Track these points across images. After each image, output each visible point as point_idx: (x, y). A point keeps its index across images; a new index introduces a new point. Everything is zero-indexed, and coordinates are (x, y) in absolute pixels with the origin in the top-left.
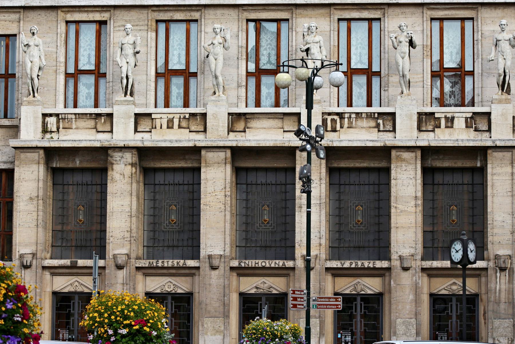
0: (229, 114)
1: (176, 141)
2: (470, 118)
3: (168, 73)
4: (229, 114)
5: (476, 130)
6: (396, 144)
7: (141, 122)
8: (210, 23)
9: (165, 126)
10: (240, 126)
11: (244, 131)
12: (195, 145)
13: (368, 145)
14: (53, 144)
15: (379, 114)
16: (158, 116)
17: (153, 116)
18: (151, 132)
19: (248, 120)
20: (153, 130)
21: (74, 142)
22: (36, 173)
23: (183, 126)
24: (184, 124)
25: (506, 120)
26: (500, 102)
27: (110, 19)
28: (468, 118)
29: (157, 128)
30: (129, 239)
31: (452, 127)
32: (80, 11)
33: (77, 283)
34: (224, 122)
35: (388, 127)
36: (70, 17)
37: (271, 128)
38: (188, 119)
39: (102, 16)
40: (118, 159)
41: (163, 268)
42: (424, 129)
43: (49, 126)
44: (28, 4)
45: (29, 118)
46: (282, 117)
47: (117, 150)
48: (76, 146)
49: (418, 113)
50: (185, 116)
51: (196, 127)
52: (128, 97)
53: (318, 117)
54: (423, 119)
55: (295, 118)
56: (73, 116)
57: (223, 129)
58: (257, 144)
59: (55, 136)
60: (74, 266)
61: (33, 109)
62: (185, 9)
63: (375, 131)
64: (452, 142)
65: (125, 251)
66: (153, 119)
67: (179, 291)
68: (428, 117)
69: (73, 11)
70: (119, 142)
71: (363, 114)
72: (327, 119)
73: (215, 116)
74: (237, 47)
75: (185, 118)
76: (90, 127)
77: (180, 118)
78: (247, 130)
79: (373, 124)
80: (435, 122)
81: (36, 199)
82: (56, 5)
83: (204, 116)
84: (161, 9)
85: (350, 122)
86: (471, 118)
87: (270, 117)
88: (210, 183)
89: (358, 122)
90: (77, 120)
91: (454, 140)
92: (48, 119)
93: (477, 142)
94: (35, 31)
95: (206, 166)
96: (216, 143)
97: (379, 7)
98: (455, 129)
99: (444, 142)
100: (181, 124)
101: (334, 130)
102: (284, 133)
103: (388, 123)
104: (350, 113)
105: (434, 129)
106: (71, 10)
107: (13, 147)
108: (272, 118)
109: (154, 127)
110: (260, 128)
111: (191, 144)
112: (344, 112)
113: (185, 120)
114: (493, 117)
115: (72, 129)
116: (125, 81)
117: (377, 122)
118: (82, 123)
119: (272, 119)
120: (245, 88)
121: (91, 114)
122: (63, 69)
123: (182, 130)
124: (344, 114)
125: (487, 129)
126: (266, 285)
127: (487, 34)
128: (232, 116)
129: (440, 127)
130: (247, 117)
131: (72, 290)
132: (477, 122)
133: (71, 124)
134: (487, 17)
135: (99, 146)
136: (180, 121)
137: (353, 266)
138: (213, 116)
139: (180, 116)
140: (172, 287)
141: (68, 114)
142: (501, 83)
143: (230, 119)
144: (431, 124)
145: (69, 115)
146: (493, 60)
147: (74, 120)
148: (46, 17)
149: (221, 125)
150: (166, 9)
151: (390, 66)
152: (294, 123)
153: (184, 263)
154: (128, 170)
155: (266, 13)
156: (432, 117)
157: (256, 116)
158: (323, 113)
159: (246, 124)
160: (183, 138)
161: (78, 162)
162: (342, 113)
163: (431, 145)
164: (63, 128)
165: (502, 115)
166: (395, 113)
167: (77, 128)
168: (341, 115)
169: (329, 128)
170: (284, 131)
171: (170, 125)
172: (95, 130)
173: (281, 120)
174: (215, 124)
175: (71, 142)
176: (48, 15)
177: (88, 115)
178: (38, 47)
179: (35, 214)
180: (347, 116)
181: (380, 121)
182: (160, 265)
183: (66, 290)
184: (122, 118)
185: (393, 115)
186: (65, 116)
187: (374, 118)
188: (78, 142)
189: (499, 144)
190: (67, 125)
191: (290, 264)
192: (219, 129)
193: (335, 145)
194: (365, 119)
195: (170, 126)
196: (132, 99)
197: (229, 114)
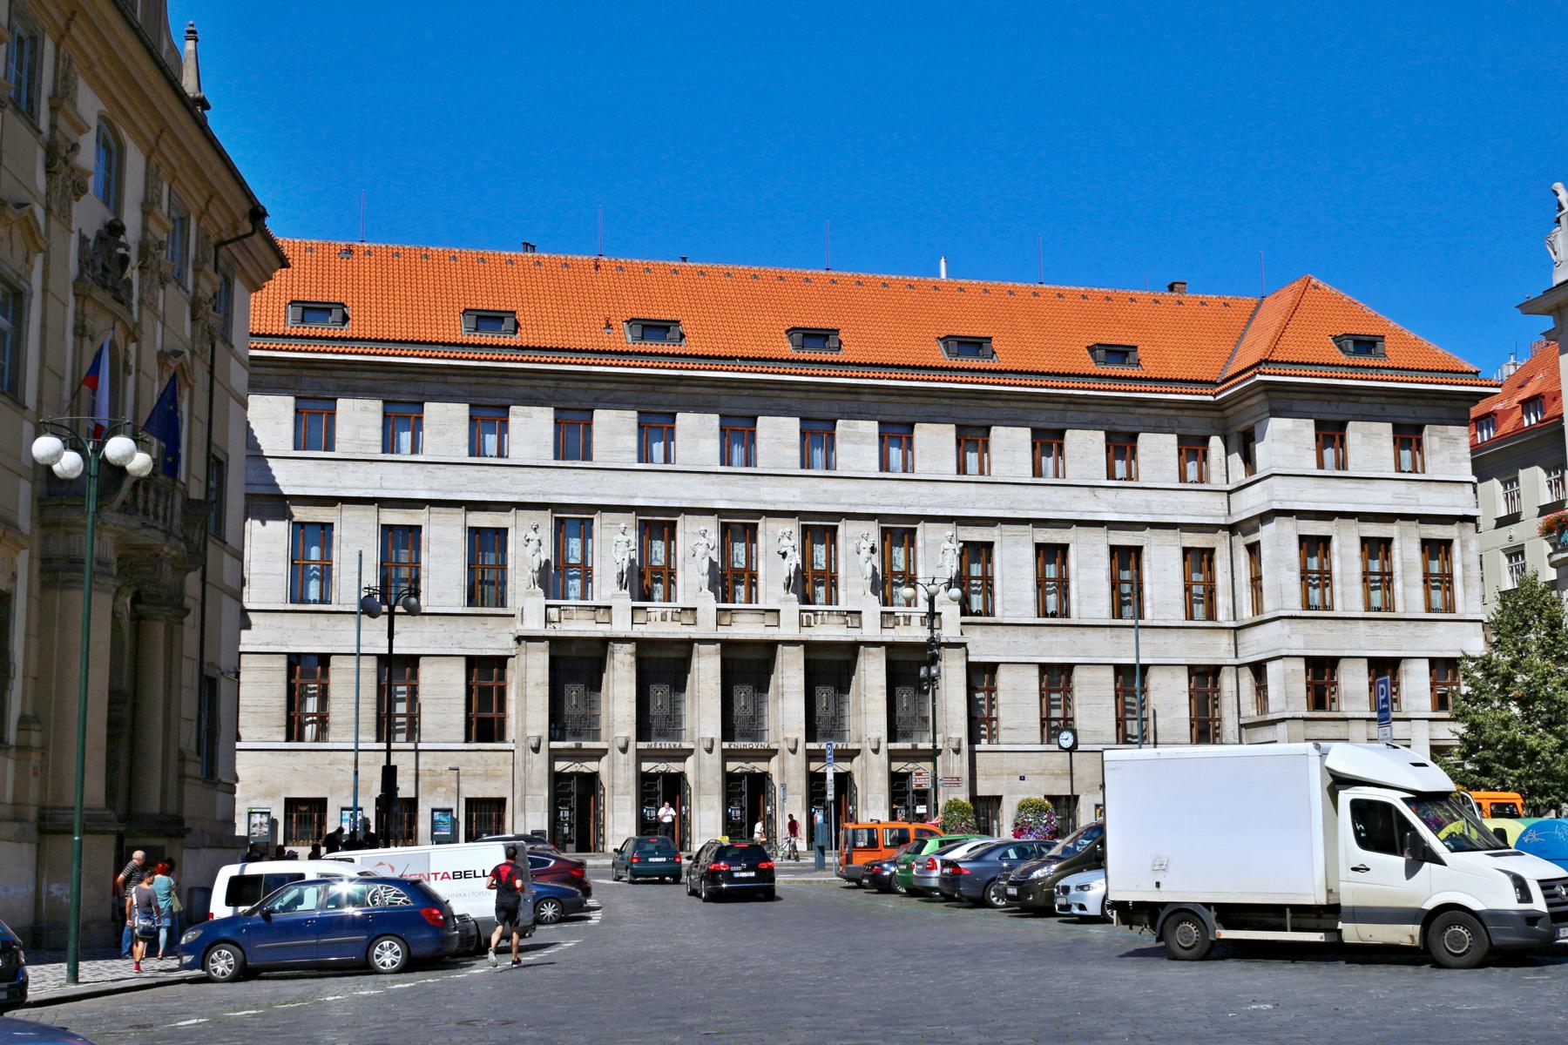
9: (659, 619)
10: (726, 620)
24: (676, 617)
55: (775, 614)
59: (557, 626)
65: (626, 735)
67: (673, 771)
85: (823, 619)
92: (549, 610)
101: (809, 626)
111: (686, 636)
129: (899, 624)
160: (675, 630)
161: (574, 650)
181: (848, 618)
182: (658, 747)
189: (952, 640)
190: (568, 616)
195: (664, 618)
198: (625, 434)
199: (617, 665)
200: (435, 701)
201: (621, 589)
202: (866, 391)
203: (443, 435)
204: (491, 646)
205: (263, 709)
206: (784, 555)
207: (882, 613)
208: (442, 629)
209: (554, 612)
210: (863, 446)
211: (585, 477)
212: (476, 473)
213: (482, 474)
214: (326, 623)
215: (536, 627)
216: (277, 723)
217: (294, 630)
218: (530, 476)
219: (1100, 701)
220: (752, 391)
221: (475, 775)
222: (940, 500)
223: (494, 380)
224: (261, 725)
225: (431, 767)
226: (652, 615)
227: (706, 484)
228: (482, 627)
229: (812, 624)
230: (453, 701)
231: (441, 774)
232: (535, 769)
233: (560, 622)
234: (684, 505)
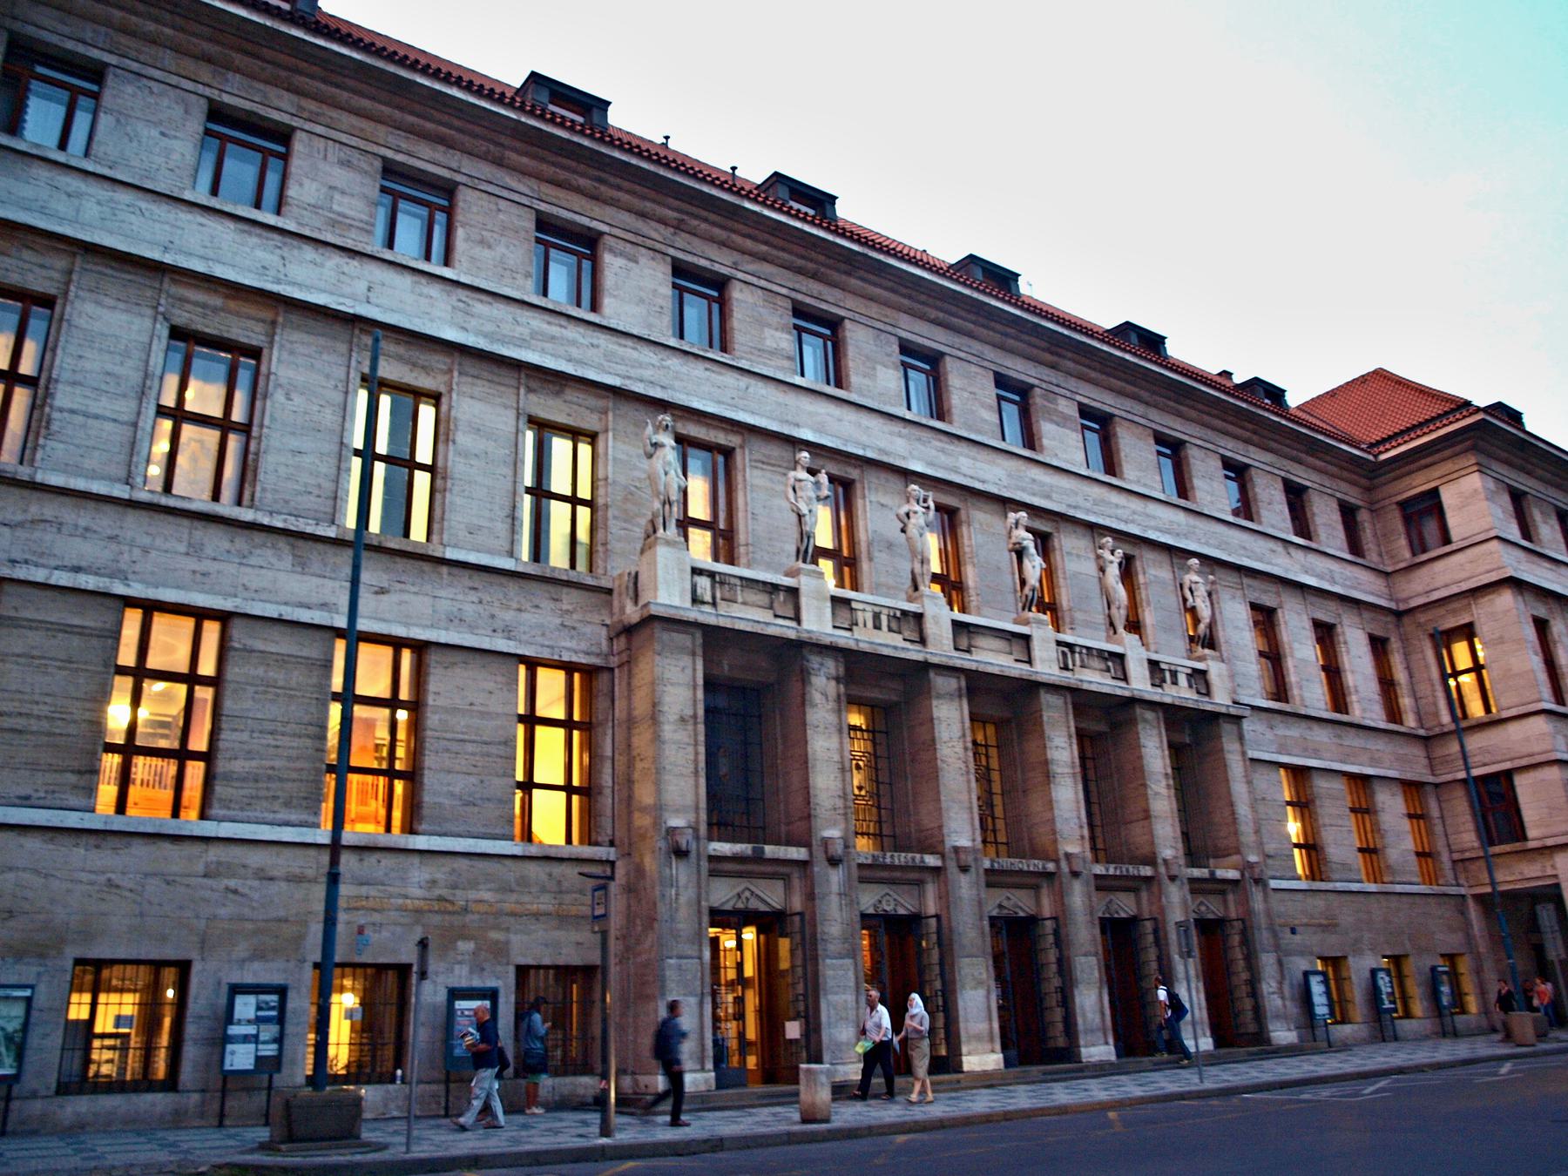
9: (870, 624)
11: (968, 651)
14: (723, 622)
17: (854, 605)
20: (855, 628)
22: (689, 671)
24: (894, 625)
30: (841, 811)
32: (699, 422)
33: (747, 894)
40: (816, 666)
41: (892, 867)
47: (815, 649)
55: (1022, 642)
56: (738, 582)
60: (758, 858)
66: (852, 609)
67: (901, 911)
75: (895, 616)
76: (760, 603)
79: (1103, 666)
81: (691, 721)
85: (1082, 661)
88: (944, 725)
95: (939, 697)
121: (764, 583)
126: (1012, 902)
131: (740, 905)
133: (735, 594)
137: (1118, 873)
140: (892, 903)
153: (922, 861)
154: (832, 688)
161: (726, 667)
164: (723, 599)
167: (744, 603)
175: (751, 624)
179: (691, 749)
180: (1077, 649)
182: (888, 860)
183: (728, 907)
190: (727, 595)
191: (1051, 867)
198: (777, 329)
199: (817, 697)
200: (455, 747)
202: (1070, 355)
203: (490, 247)
204: (568, 644)
205: (45, 725)
208: (473, 597)
209: (704, 583)
210: (1068, 432)
211: (721, 378)
212: (545, 326)
213: (554, 330)
214: (226, 545)
215: (676, 602)
216: (76, 764)
217: (145, 551)
218: (635, 354)
219: (1340, 822)
220: (941, 315)
221: (537, 916)
222: (1153, 523)
223: (583, 182)
224: (33, 766)
225: (444, 892)
226: (860, 615)
227: (891, 434)
228: (552, 605)
229: (1071, 666)
230: (493, 750)
231: (465, 910)
232: (683, 899)
233: (714, 604)
234: (870, 454)
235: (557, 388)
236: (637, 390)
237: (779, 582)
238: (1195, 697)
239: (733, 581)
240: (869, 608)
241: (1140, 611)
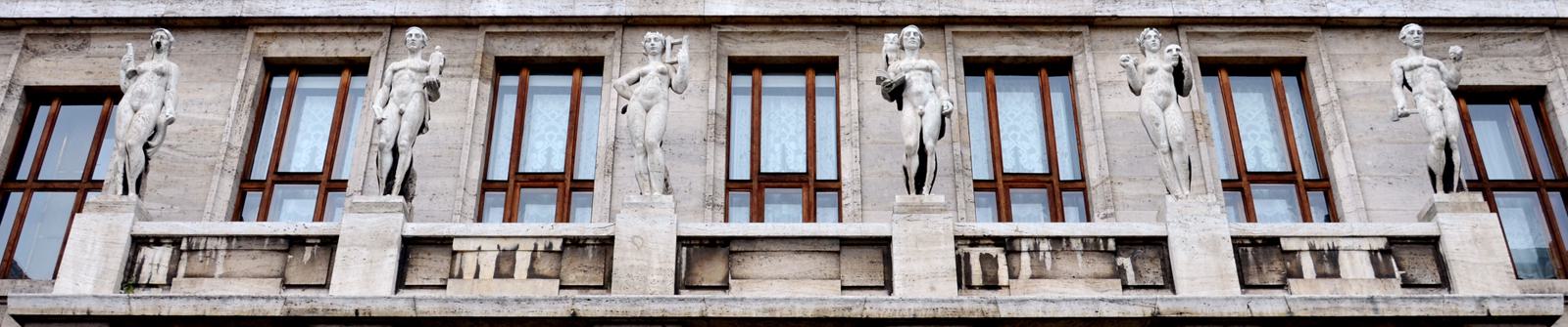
0: (680, 239)
1: (518, 301)
2: (1381, 251)
3: (516, 181)
4: (680, 239)
5: (1407, 284)
6: (1189, 310)
7: (419, 262)
8: (636, 62)
9: (488, 271)
10: (713, 270)
11: (725, 287)
12: (574, 313)
13: (1106, 315)
15: (1119, 240)
16: (472, 245)
17: (457, 245)
18: (444, 287)
19: (736, 257)
20: (450, 282)
21: (205, 302)
23: (541, 273)
24: (545, 265)
25: (1491, 252)
26: (1458, 208)
27: (377, 55)
28: (1376, 251)
29: (465, 277)
31: (1337, 275)
34: (663, 259)
35: (1151, 276)
36: (278, 49)
37: (802, 278)
38: (560, 253)
39: (360, 48)
42: (1256, 281)
43: (146, 269)
44: (173, 13)
45: (89, 247)
46: (837, 248)
48: (208, 314)
49: (1232, 238)
50: (551, 245)
51: (582, 274)
52: (395, 198)
53: (943, 247)
54: (1247, 256)
55: (876, 254)
56: (223, 244)
57: (661, 278)
58: (765, 311)
61: (110, 222)
62: (574, 29)
63: (1113, 285)
64: (1357, 305)
66: (454, 253)
68: (1260, 249)
69: (284, 35)
70: (341, 302)
71: (1073, 241)
72: (967, 255)
73: (639, 242)
74: (705, 116)
75: (549, 250)
76: (265, 272)
77: (535, 251)
78: (731, 281)
79: (1102, 266)
80: (1285, 264)
82: (244, 15)
83: (606, 244)
84: (511, 29)
86: (1386, 252)
87: (801, 248)
89: (1058, 262)
90: (233, 253)
91: (1361, 300)
92: (147, 252)
93: (1431, 305)
94: (164, 42)
96: (640, 309)
97: (1066, 29)
98: (1347, 280)
99: (1335, 304)
100: (535, 266)
101: (991, 285)
102: (844, 292)
103: (1148, 265)
104: (1035, 238)
105: (1284, 280)
106: (281, 30)
107: (13, 316)
108: (805, 251)
109: (456, 273)
110: (772, 278)
112: (1018, 234)
113: (548, 256)
114: (1448, 247)
115: (213, 277)
116: (388, 160)
117: (1115, 263)
118: (243, 262)
119: (807, 255)
120: (722, 210)
122: (235, 163)
123: (540, 282)
124: (1016, 242)
125: (1438, 280)
127: (1348, 89)
128: (688, 246)
129: (1301, 276)
130: (735, 248)
132: (1405, 263)
133: (213, 266)
134: (1341, 55)
135: (277, 314)
136: (533, 259)
138: (633, 242)
139: (536, 245)
141: (207, 237)
142: (1439, 171)
143: (684, 256)
144: (1273, 267)
145: (209, 241)
146: (1407, 115)
147: (222, 254)
148: (215, 48)
149: (656, 266)
150: (524, 29)
151: (1112, 158)
152: (872, 267)
155: (779, 44)
156: (1275, 251)
157: (760, 245)
158: (957, 238)
159: (729, 269)
162: (1012, 238)
163: (1297, 314)
164: (187, 276)
165: (1476, 240)
166: (1165, 239)
167: (226, 276)
168: (1008, 244)
169: (977, 279)
170: (844, 288)
171: (505, 269)
172: (280, 280)
173: (832, 259)
174: (636, 263)
175: (193, 302)
176: (222, 43)
177: (267, 241)
178: (164, 79)
180: (1025, 245)
181: (1125, 261)
184: (364, 246)
185: (1159, 243)
186: (198, 244)
187: (1106, 251)
188: (214, 303)
190: (197, 268)
192: (650, 278)
193: (1004, 315)
194: (1079, 256)
196: (401, 199)
197: (681, 240)
201: (388, 191)
206: (896, 93)
207: (1238, 242)
226: (469, 264)
229: (1003, 277)
233: (169, 284)
235: (78, 42)
236: (190, 14)
237: (301, 232)
238: (1400, 292)
239: (212, 244)
240: (485, 244)
241: (1326, 156)
